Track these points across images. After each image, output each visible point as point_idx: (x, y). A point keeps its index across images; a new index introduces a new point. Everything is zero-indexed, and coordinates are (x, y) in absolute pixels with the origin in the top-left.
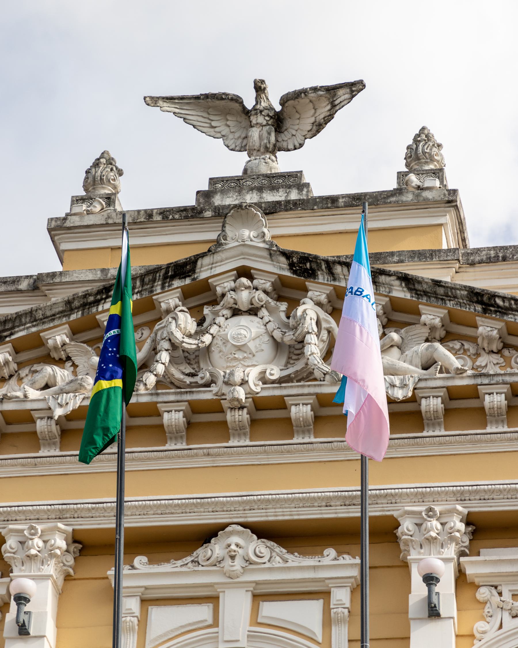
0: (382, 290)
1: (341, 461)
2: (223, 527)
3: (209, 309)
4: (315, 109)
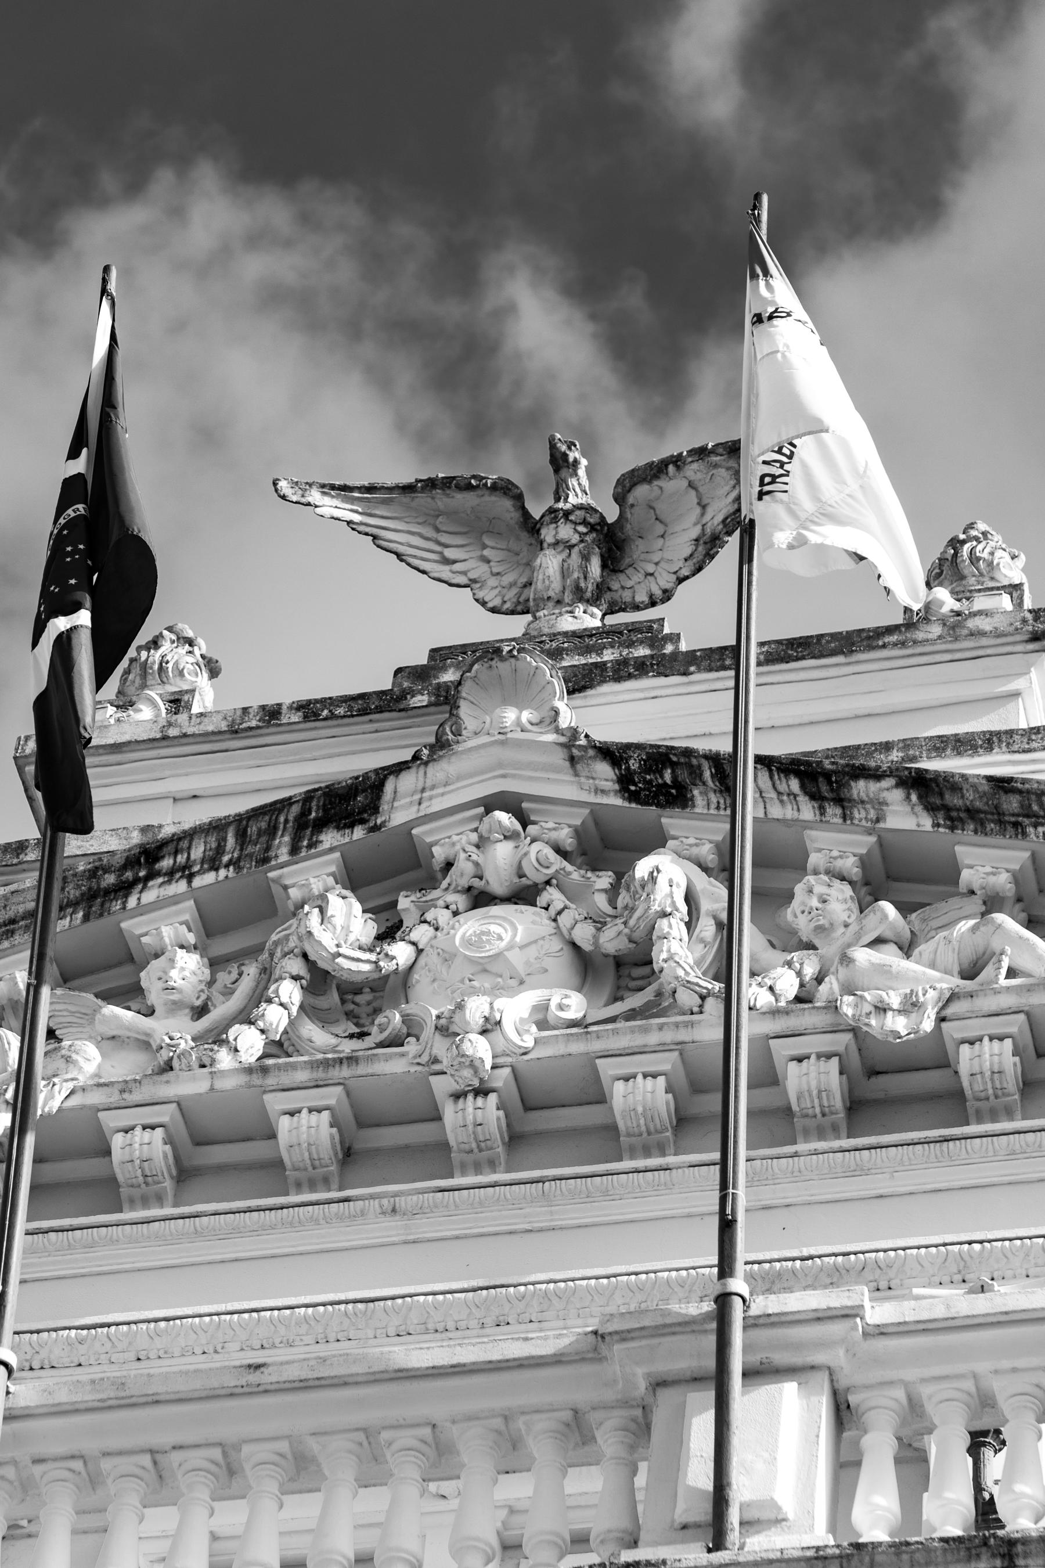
0: (858, 814)
3: (413, 898)
4: (704, 507)
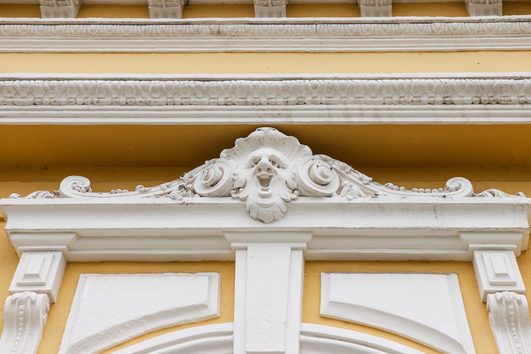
1: (449, 52)
2: (245, 131)
